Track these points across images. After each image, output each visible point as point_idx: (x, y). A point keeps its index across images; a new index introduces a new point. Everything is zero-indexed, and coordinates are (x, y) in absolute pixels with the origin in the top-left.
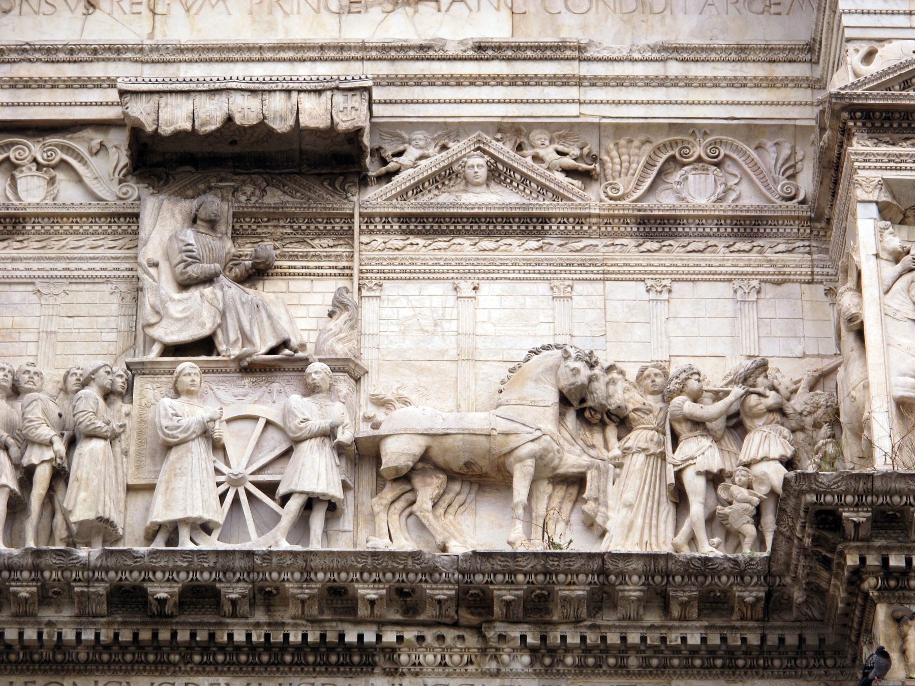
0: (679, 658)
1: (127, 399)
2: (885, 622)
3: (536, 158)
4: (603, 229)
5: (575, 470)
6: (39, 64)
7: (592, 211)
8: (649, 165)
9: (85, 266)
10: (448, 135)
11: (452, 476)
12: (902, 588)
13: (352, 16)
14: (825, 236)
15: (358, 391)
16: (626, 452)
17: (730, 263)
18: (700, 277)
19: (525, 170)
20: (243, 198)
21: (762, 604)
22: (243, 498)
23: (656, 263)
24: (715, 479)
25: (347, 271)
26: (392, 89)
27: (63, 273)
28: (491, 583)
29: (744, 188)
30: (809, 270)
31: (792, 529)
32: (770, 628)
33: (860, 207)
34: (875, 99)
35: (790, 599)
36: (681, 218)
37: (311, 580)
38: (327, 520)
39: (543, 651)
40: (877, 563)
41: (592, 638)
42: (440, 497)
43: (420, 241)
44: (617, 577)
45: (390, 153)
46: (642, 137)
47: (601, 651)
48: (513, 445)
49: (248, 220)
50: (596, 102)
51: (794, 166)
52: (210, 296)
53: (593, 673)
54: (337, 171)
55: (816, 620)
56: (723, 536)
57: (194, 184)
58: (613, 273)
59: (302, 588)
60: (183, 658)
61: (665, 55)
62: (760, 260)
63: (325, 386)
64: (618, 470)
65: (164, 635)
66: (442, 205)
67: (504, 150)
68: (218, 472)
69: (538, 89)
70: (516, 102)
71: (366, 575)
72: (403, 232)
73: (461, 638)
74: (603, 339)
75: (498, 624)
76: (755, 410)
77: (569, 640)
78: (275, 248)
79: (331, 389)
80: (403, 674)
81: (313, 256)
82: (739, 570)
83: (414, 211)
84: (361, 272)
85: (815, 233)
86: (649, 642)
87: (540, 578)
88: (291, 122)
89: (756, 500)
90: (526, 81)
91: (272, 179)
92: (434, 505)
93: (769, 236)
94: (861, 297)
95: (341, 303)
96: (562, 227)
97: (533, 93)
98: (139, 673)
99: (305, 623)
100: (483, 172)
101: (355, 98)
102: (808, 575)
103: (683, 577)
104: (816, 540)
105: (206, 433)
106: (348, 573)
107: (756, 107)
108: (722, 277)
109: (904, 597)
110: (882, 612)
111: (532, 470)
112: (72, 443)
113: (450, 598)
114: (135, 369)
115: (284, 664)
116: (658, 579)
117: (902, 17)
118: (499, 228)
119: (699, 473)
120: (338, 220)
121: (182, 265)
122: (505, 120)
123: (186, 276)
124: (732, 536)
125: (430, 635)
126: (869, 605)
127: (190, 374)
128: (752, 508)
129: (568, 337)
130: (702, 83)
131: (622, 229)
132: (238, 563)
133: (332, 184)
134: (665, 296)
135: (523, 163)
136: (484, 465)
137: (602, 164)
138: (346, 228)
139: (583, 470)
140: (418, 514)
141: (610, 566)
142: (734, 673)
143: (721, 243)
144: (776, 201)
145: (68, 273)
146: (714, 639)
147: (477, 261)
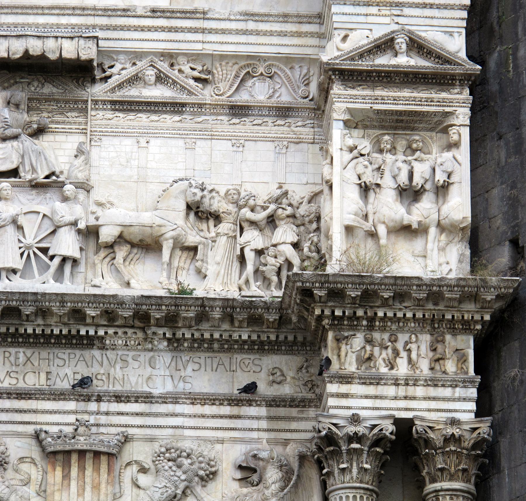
0: (237, 345)
2: (332, 341)
3: (180, 71)
4: (212, 111)
5: (193, 244)
7: (207, 102)
8: (237, 76)
10: (136, 57)
11: (133, 245)
12: (341, 325)
14: (321, 118)
15: (88, 197)
16: (218, 234)
17: (273, 132)
18: (259, 139)
19: (174, 78)
20: (33, 89)
21: (277, 322)
23: (237, 131)
25: (84, 131)
26: (109, 31)
28: (150, 309)
29: (283, 90)
30: (312, 137)
31: (291, 293)
32: (281, 332)
33: (335, 123)
34: (345, 66)
35: (291, 319)
36: (251, 106)
37: (64, 306)
38: (72, 266)
39: (174, 340)
40: (329, 314)
41: (197, 335)
42: (127, 256)
43: (121, 115)
44: (209, 308)
45: (107, 66)
47: (201, 341)
48: (163, 232)
49: (35, 101)
50: (211, 42)
51: (308, 79)
52: (17, 147)
53: (197, 350)
54: (80, 75)
55: (302, 329)
56: (262, 280)
57: (8, 80)
58: (216, 135)
59: (60, 310)
61: (246, 17)
62: (289, 131)
63: (72, 197)
64: (213, 244)
67: (164, 66)
68: (20, 241)
69: (182, 34)
70: (171, 41)
71: (90, 305)
72: (113, 110)
73: (135, 333)
74: (209, 172)
75: (152, 327)
76: (281, 217)
77: (186, 336)
78: (49, 117)
79: (75, 197)
80: (107, 349)
81: (68, 122)
82: (267, 306)
83: (118, 99)
84: (91, 131)
85: (317, 116)
86: (223, 338)
87: (173, 308)
88: (58, 55)
89: (278, 265)
91: (48, 78)
92: (124, 260)
93: (294, 117)
94: (332, 168)
95: (81, 150)
96: (192, 110)
97: (180, 36)
99: (61, 325)
100: (153, 79)
101: (90, 42)
102: (298, 312)
103: (240, 309)
104: (301, 300)
105: (14, 221)
106: (82, 303)
107: (291, 47)
108: (269, 139)
109: (341, 328)
110: (330, 335)
111: (172, 245)
113: (130, 316)
115: (51, 343)
116: (229, 309)
117: (362, 17)
118: (160, 109)
119: (252, 250)
120: (80, 103)
121: (2, 129)
122: (165, 51)
123: (4, 135)
124: (266, 281)
125: (120, 331)
126: (325, 331)
127: (6, 190)
128: (276, 269)
129: (192, 170)
130: (265, 33)
131: (222, 111)
132: (30, 298)
133: (77, 82)
134: (241, 149)
135: (174, 74)
136: (149, 241)
138: (84, 107)
139: (196, 244)
140: (116, 265)
141: (206, 303)
142: (263, 352)
143: (270, 120)
144: (299, 99)
146: (254, 337)
147: (149, 128)
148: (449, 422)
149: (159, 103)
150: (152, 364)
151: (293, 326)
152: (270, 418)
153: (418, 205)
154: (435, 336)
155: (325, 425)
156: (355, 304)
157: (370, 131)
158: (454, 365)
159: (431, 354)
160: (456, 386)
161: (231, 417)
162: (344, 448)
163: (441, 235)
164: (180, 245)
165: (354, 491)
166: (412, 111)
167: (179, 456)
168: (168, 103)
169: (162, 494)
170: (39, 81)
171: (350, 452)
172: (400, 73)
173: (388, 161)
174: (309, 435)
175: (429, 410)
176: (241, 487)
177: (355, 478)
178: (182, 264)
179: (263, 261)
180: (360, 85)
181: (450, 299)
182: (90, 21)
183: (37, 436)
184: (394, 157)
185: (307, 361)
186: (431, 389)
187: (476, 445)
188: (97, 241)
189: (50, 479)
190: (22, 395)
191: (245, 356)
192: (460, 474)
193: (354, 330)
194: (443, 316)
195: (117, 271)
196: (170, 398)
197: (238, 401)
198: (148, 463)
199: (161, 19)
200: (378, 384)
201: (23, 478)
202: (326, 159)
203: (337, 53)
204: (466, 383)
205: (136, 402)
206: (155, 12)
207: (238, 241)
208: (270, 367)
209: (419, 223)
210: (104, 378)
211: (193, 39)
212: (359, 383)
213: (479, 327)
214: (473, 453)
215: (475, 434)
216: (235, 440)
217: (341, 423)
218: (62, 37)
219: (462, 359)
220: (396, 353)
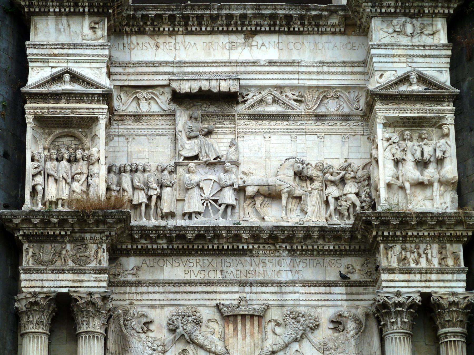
1: (175, 173)
3: (286, 96)
6: (144, 67)
8: (318, 98)
9: (160, 131)
11: (265, 196)
13: (233, 50)
15: (238, 170)
16: (312, 189)
20: (204, 109)
22: (209, 204)
26: (245, 75)
27: (154, 133)
33: (378, 125)
35: (357, 237)
36: (327, 115)
41: (304, 247)
42: (262, 203)
43: (254, 122)
46: (316, 89)
48: (282, 189)
51: (359, 98)
60: (195, 252)
63: (230, 170)
65: (191, 247)
66: (259, 111)
72: (249, 119)
73: (270, 247)
77: (298, 248)
80: (254, 256)
82: (344, 230)
87: (291, 232)
88: (218, 90)
90: (283, 73)
93: (352, 120)
94: (377, 151)
97: (286, 76)
98: (184, 256)
100: (271, 101)
104: (365, 227)
110: (382, 246)
113: (267, 238)
114: (177, 164)
116: (322, 232)
119: (332, 198)
125: (261, 246)
126: (378, 244)
128: (347, 208)
130: (334, 73)
134: (323, 140)
135: (283, 98)
136: (274, 194)
137: (305, 98)
143: (338, 123)
145: (156, 133)
146: (337, 247)
147: (270, 129)
148: (451, 294)
149: (275, 115)
150: (280, 264)
151: (358, 241)
152: (347, 293)
153: (427, 170)
154: (441, 245)
155: (382, 298)
156: (395, 228)
157: (398, 129)
158: (452, 261)
159: (439, 256)
160: (454, 273)
161: (326, 293)
162: (392, 310)
163: (441, 187)
164: (291, 196)
165: (399, 334)
166: (421, 117)
167: (298, 316)
168: (280, 115)
169: (289, 338)
170: (207, 104)
171: (397, 312)
172: (414, 95)
173: (408, 145)
174: (371, 302)
175: (440, 287)
176: (333, 333)
177: (399, 327)
178: (293, 206)
179: (339, 204)
180: (391, 103)
181: (449, 224)
182: (234, 69)
183: (218, 307)
184: (412, 143)
185: (367, 260)
186: (440, 275)
187: (467, 307)
188: (245, 195)
189: (227, 331)
191: (331, 258)
192: (459, 323)
193: (394, 243)
194: (445, 234)
195: (257, 211)
196: (291, 283)
197: (329, 284)
198: (280, 321)
199: (274, 67)
200: (410, 273)
201: (211, 331)
202: (373, 145)
203: (377, 85)
204: (459, 271)
205: (272, 286)
206: (271, 63)
207: (324, 193)
208: (346, 264)
209: (429, 180)
210: (253, 273)
211: (293, 78)
212: (399, 273)
213: (465, 239)
214: (465, 311)
215: (466, 301)
216: (328, 306)
217: (391, 296)
218: (220, 80)
219: (456, 258)
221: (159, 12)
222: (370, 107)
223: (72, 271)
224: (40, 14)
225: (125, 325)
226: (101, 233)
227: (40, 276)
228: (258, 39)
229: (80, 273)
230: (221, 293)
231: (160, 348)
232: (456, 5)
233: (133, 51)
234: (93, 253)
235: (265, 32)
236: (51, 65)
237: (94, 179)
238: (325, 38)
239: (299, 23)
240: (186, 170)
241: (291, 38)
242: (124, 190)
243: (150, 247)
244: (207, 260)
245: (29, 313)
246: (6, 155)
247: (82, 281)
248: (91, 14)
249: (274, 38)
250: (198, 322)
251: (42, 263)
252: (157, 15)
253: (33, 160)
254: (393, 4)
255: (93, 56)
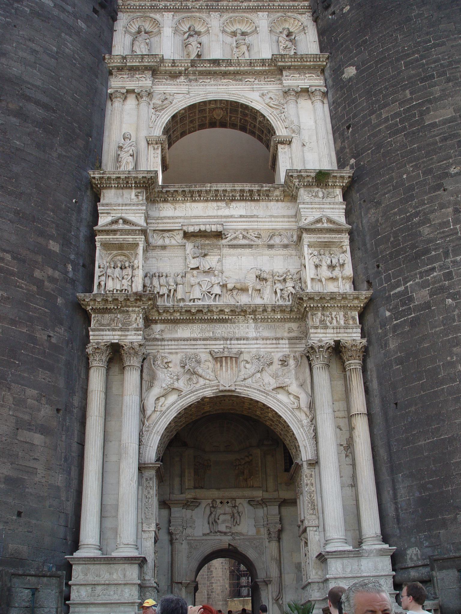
3: (250, 235)
8: (269, 236)
11: (238, 290)
24: (282, 290)
29: (285, 239)
65: (194, 318)
79: (218, 275)
88: (210, 230)
97: (250, 224)
100: (242, 237)
105: (199, 283)
110: (309, 313)
112: (177, 285)
125: (237, 317)
130: (278, 222)
135: (248, 236)
146: (282, 317)
157: (316, 249)
179: (283, 293)
190: (204, 339)
192: (357, 357)
198: (249, 360)
203: (303, 224)
205: (244, 340)
206: (241, 216)
216: (277, 352)
220: (332, 318)
221: (177, 189)
222: (300, 238)
223: (121, 330)
224: (106, 188)
225: (154, 364)
226: (139, 307)
227: (102, 333)
228: (234, 204)
229: (126, 331)
230: (212, 345)
231: (175, 377)
232: (347, 181)
233: (161, 212)
234: (134, 319)
235: (238, 200)
236: (112, 215)
237: (135, 278)
238: (272, 203)
239: (257, 195)
240: (192, 276)
241: (253, 204)
242: (154, 287)
243: (169, 318)
244: (205, 326)
245: (94, 355)
246: (84, 266)
247: (127, 335)
248: (136, 187)
249: (243, 204)
250: (199, 362)
251: (103, 325)
252: (175, 191)
253: (99, 267)
254: (311, 181)
255: (137, 210)
